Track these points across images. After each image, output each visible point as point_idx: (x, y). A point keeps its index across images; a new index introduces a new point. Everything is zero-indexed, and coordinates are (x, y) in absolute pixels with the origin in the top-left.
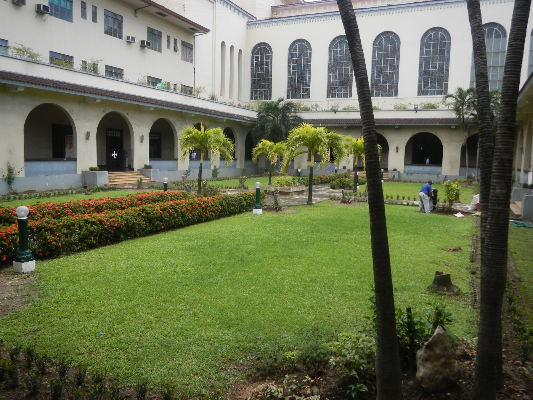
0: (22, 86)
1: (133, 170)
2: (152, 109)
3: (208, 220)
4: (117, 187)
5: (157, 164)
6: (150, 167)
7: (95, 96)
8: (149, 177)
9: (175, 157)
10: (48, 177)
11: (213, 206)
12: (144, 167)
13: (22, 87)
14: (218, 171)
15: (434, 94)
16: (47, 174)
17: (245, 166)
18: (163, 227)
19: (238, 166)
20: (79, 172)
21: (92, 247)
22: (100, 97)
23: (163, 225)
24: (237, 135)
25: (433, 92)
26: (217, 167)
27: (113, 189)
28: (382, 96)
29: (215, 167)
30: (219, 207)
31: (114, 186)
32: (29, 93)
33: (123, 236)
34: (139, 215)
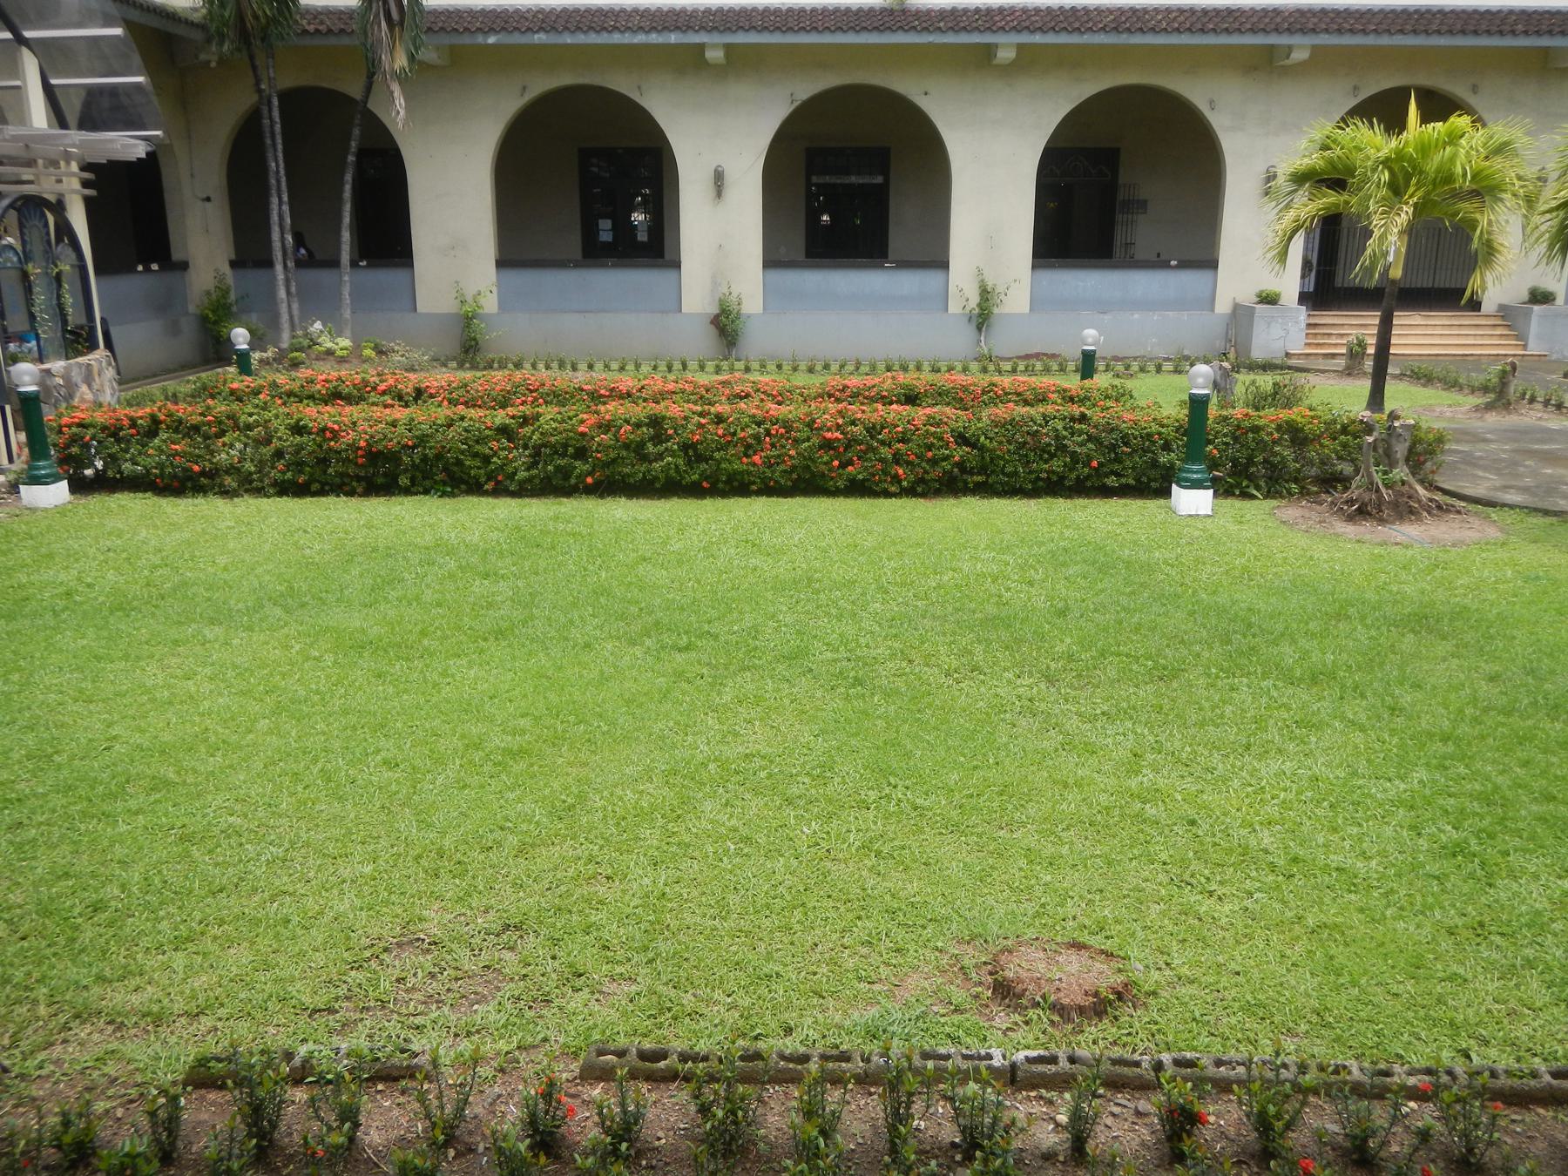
0: (1007, 47)
1: (1475, 305)
3: (858, 489)
4: (1321, 364)
7: (1284, 40)
8: (1522, 337)
10: (1107, 317)
11: (903, 441)
12: (1525, 296)
13: (1005, 45)
16: (1103, 306)
18: (589, 480)
20: (1223, 306)
21: (286, 489)
22: (1296, 40)
23: (590, 473)
30: (959, 452)
32: (1029, 63)
33: (404, 481)
34: (503, 431)
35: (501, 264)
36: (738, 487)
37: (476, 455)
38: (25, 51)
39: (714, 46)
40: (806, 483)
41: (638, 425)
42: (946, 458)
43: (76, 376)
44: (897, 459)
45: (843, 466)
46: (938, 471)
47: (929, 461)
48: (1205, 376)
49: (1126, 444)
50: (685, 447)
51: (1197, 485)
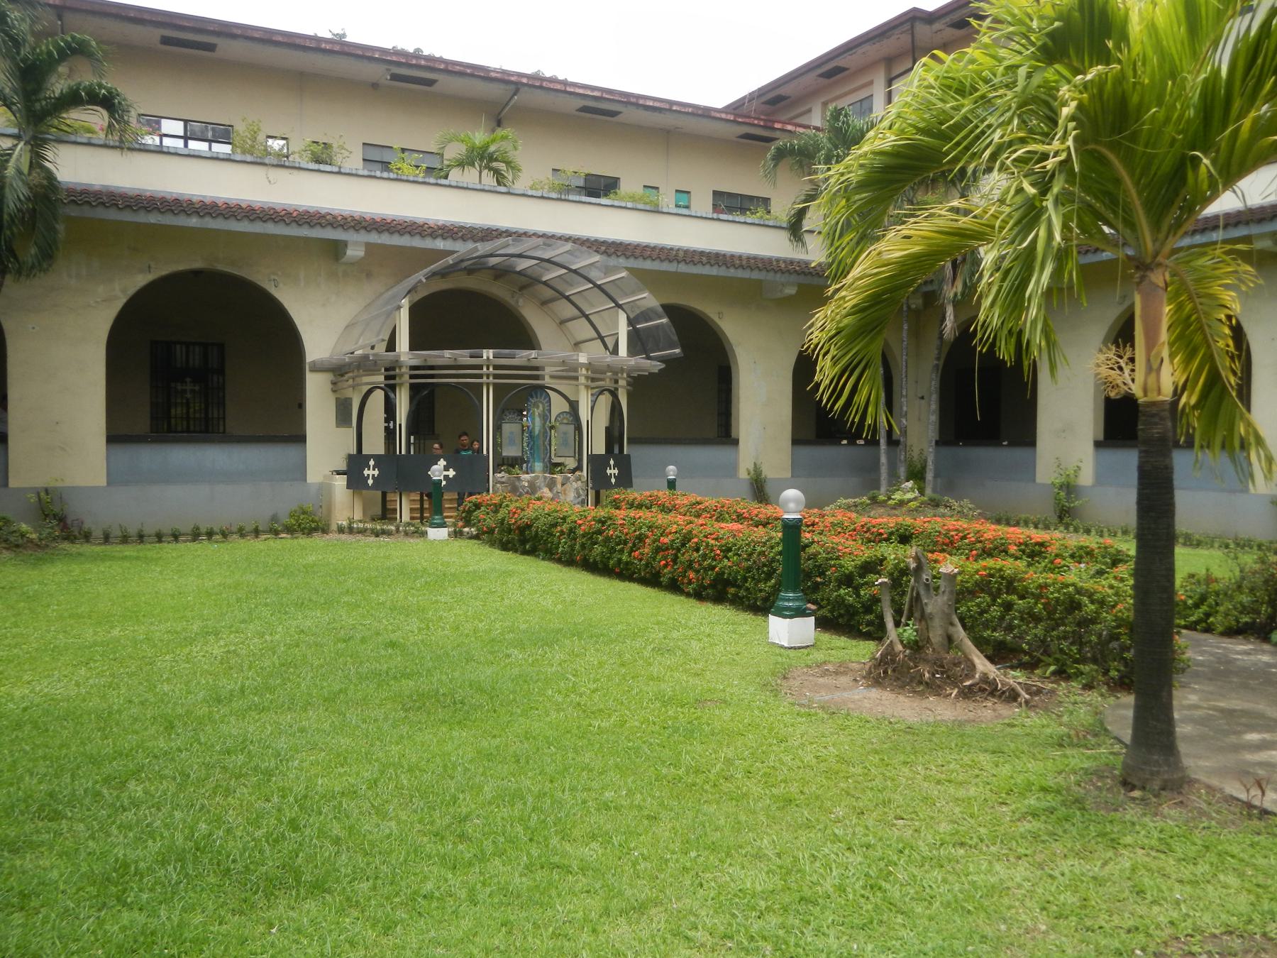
3: (674, 587)
35: (1098, 444)
36: (624, 573)
37: (551, 535)
38: (620, 311)
39: (1262, 236)
40: (652, 580)
41: (600, 521)
42: (713, 568)
43: (539, 482)
44: (690, 565)
45: (666, 566)
46: (707, 582)
47: (705, 569)
48: (796, 501)
49: (822, 574)
50: (608, 539)
51: (781, 613)
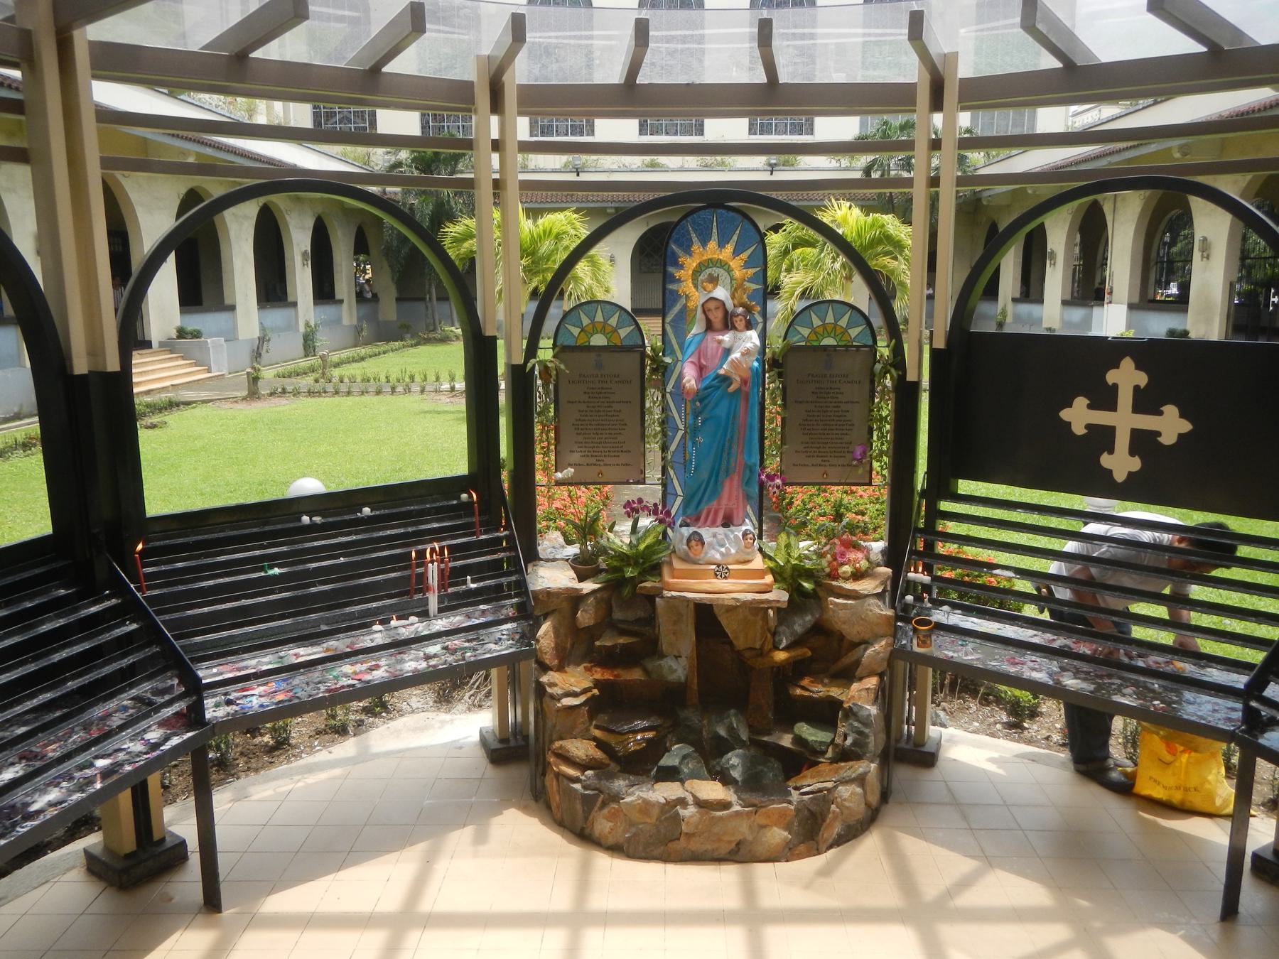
1: (147, 344)
2: (191, 160)
5: (196, 321)
6: (197, 335)
9: (227, 302)
12: (174, 334)
14: (319, 336)
15: (785, 133)
17: (359, 319)
19: (346, 321)
24: (339, 233)
25: (781, 128)
26: (312, 324)
27: (172, 405)
28: (667, 134)
29: (307, 325)
31: (164, 397)
